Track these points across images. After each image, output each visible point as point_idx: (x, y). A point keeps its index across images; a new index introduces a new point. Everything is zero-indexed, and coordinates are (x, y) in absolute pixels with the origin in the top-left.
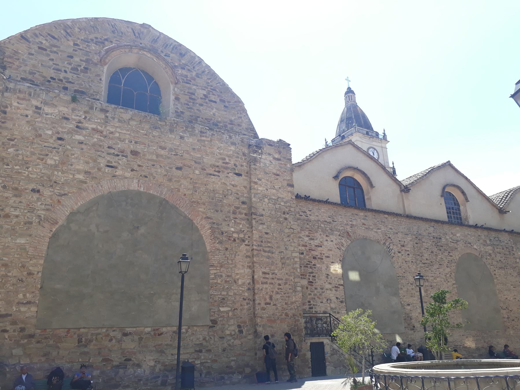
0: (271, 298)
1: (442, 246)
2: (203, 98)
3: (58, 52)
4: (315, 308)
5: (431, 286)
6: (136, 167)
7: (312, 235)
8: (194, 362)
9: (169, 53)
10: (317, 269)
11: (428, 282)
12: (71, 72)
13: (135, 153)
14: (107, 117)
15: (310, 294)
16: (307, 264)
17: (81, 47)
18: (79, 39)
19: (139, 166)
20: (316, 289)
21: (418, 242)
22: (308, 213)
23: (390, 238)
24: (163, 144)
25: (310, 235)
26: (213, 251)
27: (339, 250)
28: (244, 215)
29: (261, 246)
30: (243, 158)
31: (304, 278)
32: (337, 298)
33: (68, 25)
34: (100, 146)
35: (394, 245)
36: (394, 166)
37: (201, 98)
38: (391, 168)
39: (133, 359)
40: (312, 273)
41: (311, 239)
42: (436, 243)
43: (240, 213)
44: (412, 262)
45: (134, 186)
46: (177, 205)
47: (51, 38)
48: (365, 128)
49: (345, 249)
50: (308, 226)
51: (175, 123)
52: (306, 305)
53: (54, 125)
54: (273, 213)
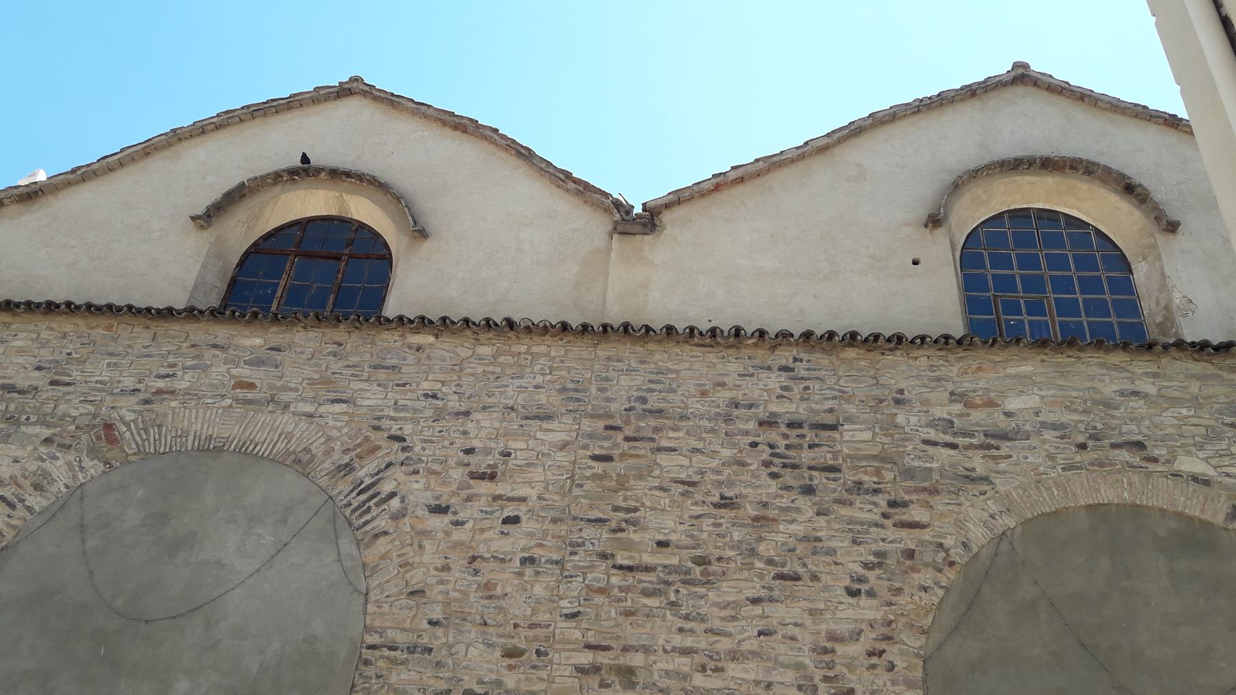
21: (616, 453)
35: (416, 472)
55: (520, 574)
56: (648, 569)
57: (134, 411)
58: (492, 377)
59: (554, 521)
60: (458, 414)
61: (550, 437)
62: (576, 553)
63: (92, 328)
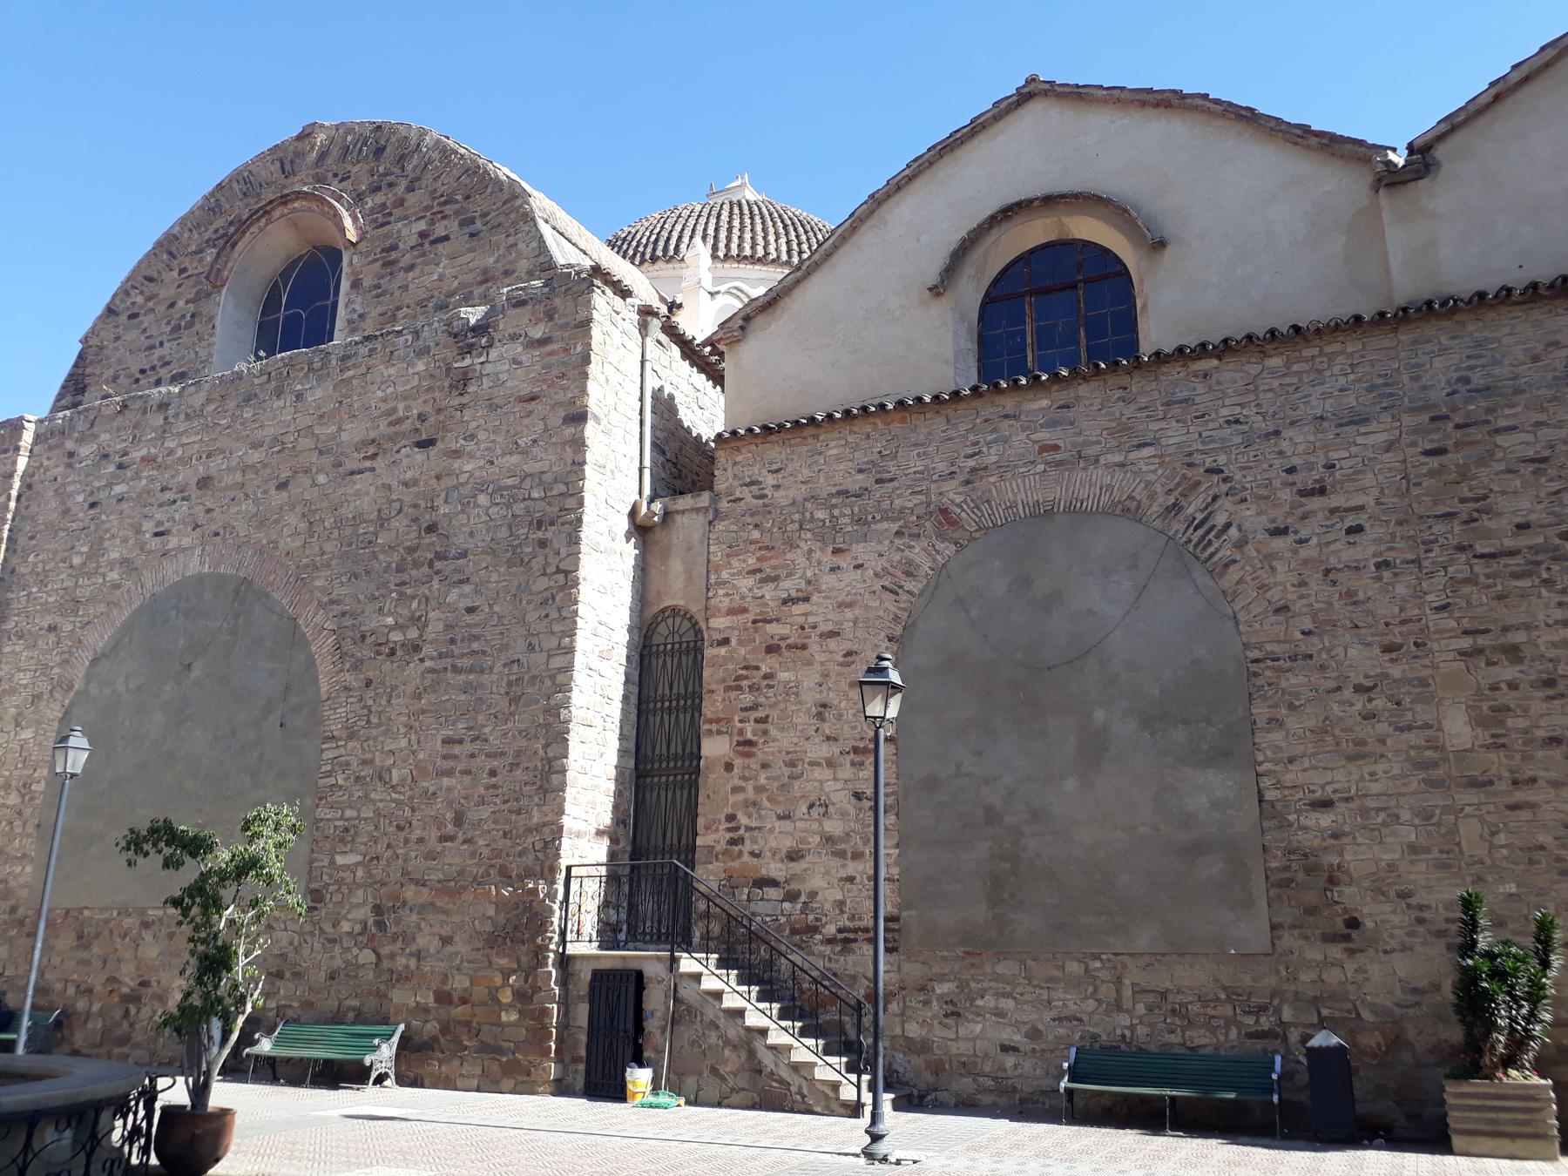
4: (754, 841)
15: (736, 790)
16: (738, 678)
20: (765, 766)
23: (1219, 471)
25: (764, 565)
27: (894, 597)
31: (719, 733)
35: (1244, 500)
40: (754, 707)
52: (717, 830)
55: (1379, 579)
56: (1512, 553)
57: (960, 493)
58: (1291, 389)
59: (1399, 523)
60: (1268, 435)
61: (1371, 440)
62: (1431, 551)
63: (889, 424)
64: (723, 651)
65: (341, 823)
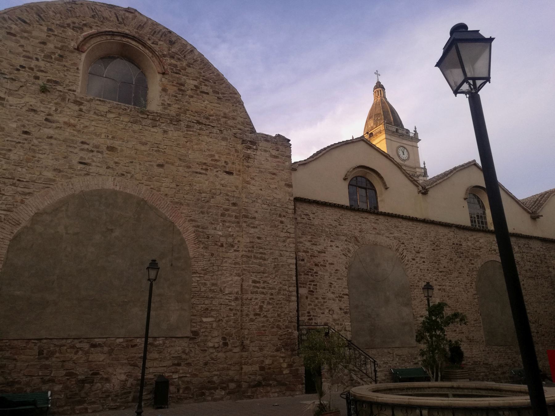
0: (261, 308)
1: (462, 253)
2: (195, 90)
3: (29, 38)
4: (315, 319)
5: (448, 296)
6: (111, 164)
7: (315, 240)
8: (171, 376)
9: (157, 40)
10: (319, 277)
11: (445, 291)
12: (43, 60)
13: (111, 149)
14: (81, 110)
15: (309, 305)
16: (308, 272)
17: (56, 33)
18: (53, 24)
19: (116, 163)
20: (317, 298)
22: (312, 216)
24: (144, 140)
26: (196, 256)
28: (233, 219)
29: (252, 251)
30: (236, 154)
31: (304, 287)
32: (341, 309)
33: (41, 8)
34: (73, 141)
35: (408, 251)
36: (425, 167)
37: (191, 89)
38: (422, 168)
39: (101, 373)
40: (313, 281)
41: (314, 244)
42: (456, 249)
43: (230, 216)
44: (428, 270)
45: (109, 184)
46: (156, 206)
47: (21, 22)
48: (395, 125)
49: (351, 255)
50: (310, 230)
51: (158, 116)
53: (19, 117)
54: (267, 215)
61: (425, 244)
64: (302, 263)
65: (204, 306)
